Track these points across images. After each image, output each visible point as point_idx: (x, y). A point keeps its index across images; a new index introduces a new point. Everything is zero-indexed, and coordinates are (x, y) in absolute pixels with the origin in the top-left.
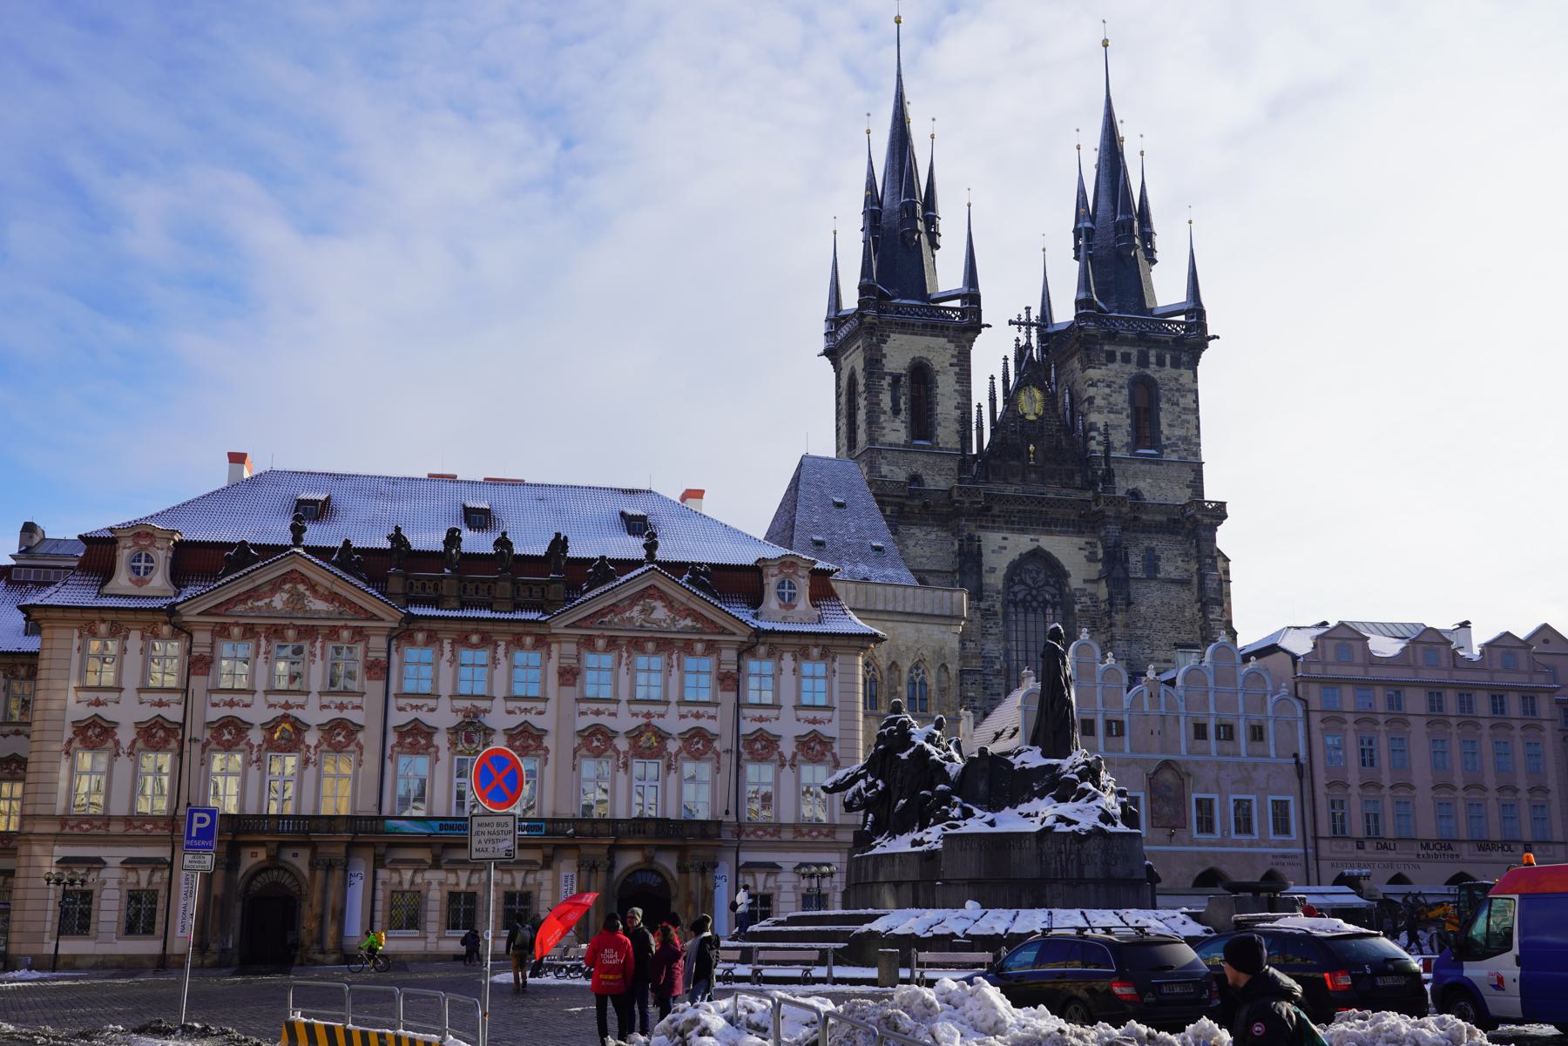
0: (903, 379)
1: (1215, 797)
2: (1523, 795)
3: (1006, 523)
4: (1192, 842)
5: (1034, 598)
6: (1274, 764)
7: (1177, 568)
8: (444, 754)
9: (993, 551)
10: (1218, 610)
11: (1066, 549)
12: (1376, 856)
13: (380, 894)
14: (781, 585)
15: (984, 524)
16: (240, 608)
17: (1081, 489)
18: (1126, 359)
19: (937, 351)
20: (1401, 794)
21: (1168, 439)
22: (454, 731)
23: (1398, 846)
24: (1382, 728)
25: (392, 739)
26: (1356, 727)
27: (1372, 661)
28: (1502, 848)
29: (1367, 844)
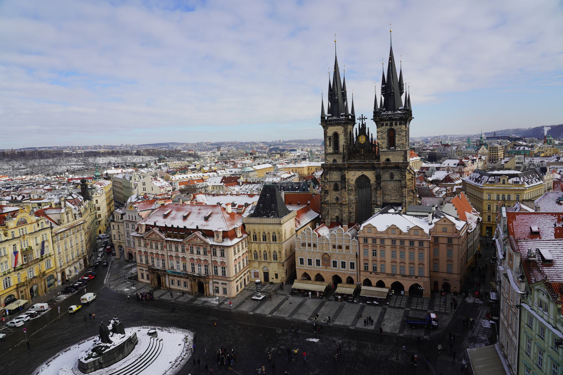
0: (331, 137)
4: (331, 269)
5: (363, 186)
8: (175, 260)
10: (405, 189)
11: (370, 175)
14: (217, 235)
17: (374, 159)
18: (387, 125)
19: (339, 129)
21: (398, 144)
25: (169, 257)
27: (377, 232)
28: (409, 277)
29: (373, 273)
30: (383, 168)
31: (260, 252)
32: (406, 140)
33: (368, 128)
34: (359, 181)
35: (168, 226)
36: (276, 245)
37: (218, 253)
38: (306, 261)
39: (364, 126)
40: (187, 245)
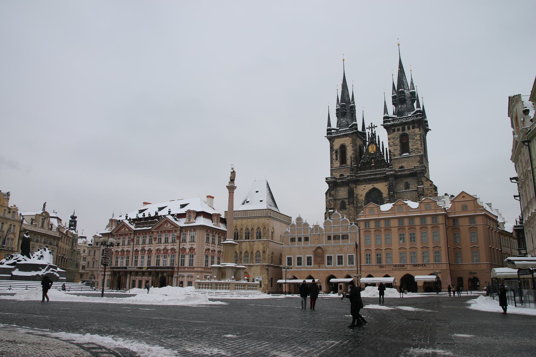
0: (338, 150)
1: (332, 255)
2: (431, 249)
3: (365, 182)
4: (326, 268)
6: (350, 245)
7: (415, 186)
8: (140, 255)
9: (362, 190)
11: (382, 187)
12: (379, 270)
13: (131, 281)
15: (359, 183)
16: (119, 232)
18: (398, 130)
19: (347, 141)
20: (388, 251)
22: (141, 251)
23: (386, 266)
24: (383, 232)
25: (134, 253)
26: (374, 232)
28: (422, 266)
30: (397, 177)
31: (241, 253)
32: (421, 144)
33: (378, 136)
34: (370, 197)
35: (140, 217)
36: (260, 243)
37: (188, 239)
38: (294, 261)
39: (374, 135)
40: (155, 234)
